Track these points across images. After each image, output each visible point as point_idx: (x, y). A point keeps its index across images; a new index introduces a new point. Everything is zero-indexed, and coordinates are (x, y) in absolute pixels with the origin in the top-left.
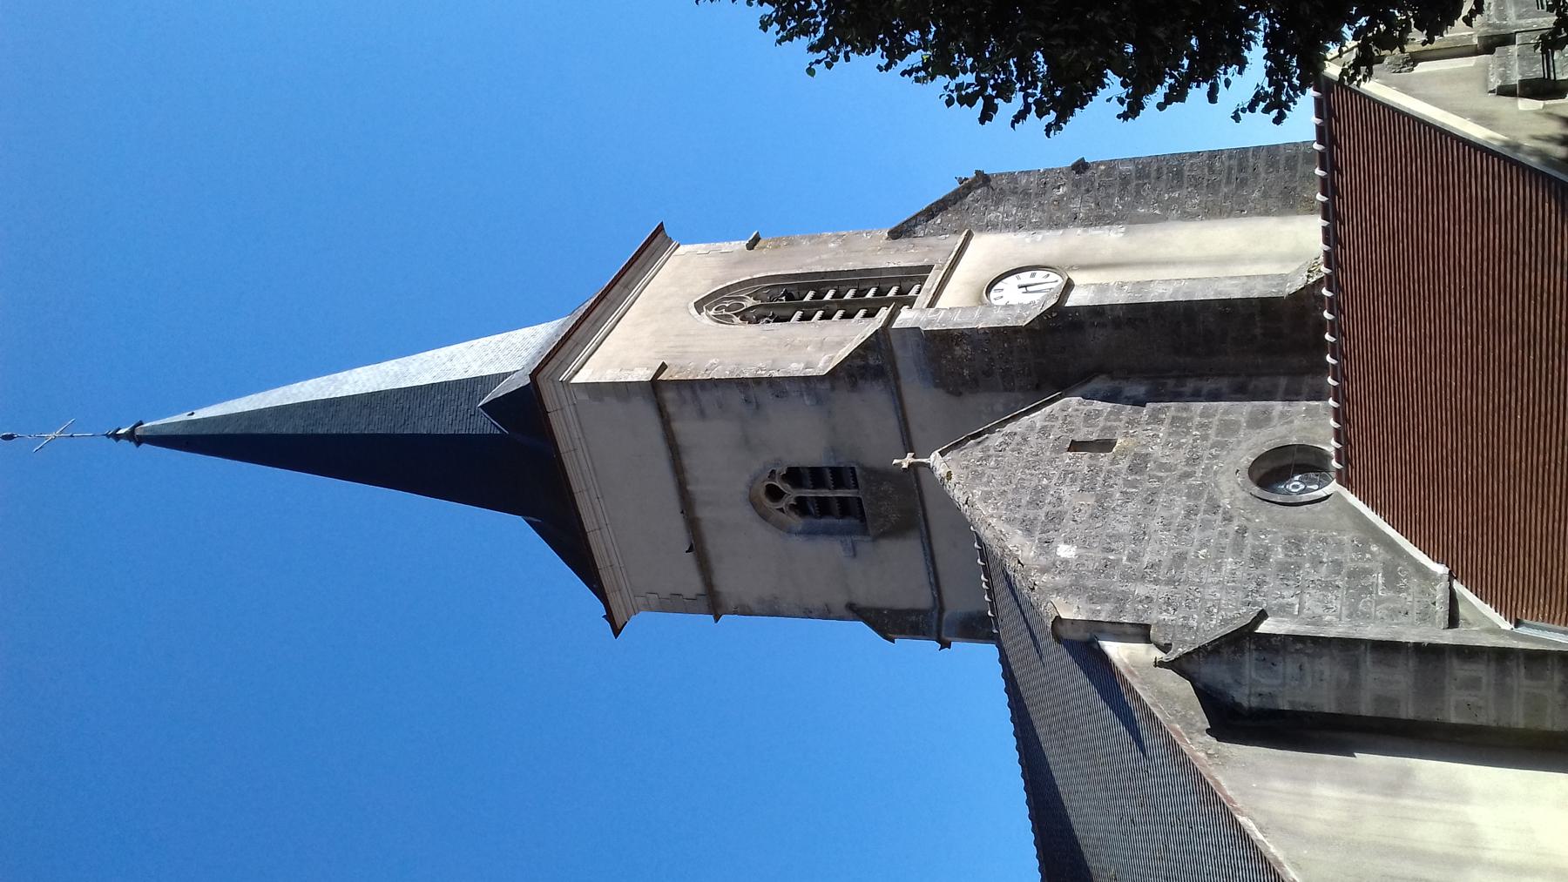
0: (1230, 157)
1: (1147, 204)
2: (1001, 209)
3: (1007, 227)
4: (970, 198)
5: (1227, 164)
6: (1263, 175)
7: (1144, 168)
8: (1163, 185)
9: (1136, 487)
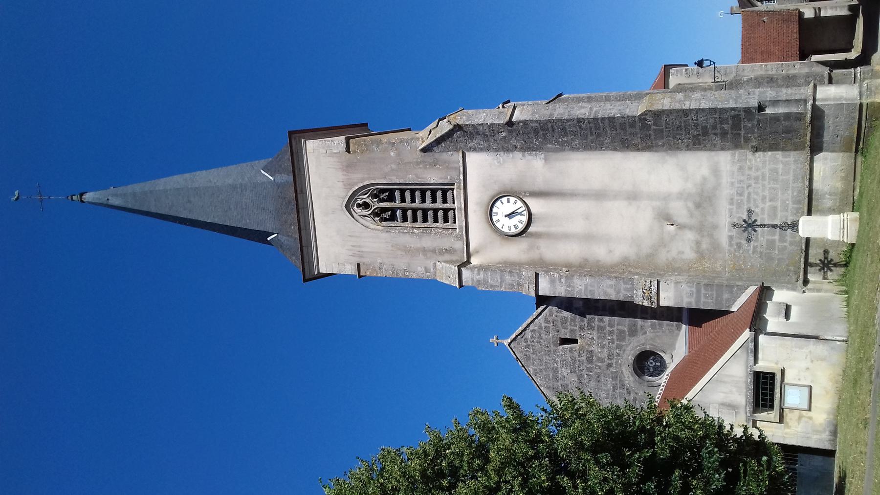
0: (589, 123)
1: (551, 143)
2: (474, 141)
3: (481, 150)
4: (455, 136)
5: (588, 126)
6: (609, 132)
7: (544, 125)
8: (557, 134)
9: (591, 372)
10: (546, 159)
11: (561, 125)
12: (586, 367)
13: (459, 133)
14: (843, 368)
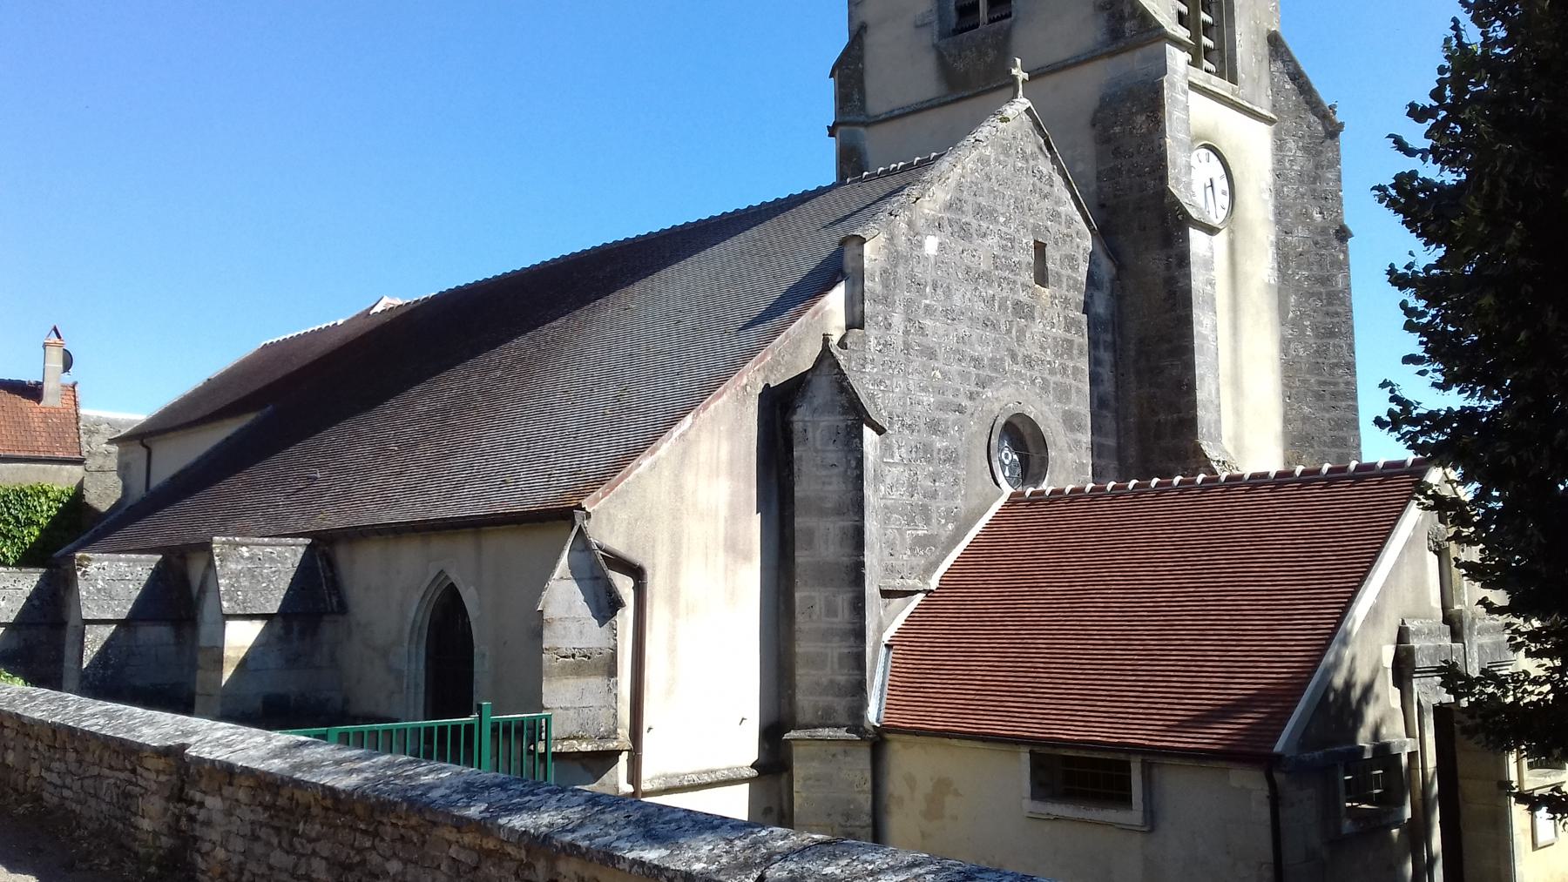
0: (1348, 383)
1: (1299, 304)
2: (1299, 153)
3: (1279, 161)
4: (1313, 118)
5: (1341, 380)
6: (1327, 416)
7: (1340, 299)
8: (1319, 319)
9: (999, 308)
10: (1269, 285)
11: (1340, 331)
12: (1007, 297)
13: (1320, 129)
14: (469, 844)
